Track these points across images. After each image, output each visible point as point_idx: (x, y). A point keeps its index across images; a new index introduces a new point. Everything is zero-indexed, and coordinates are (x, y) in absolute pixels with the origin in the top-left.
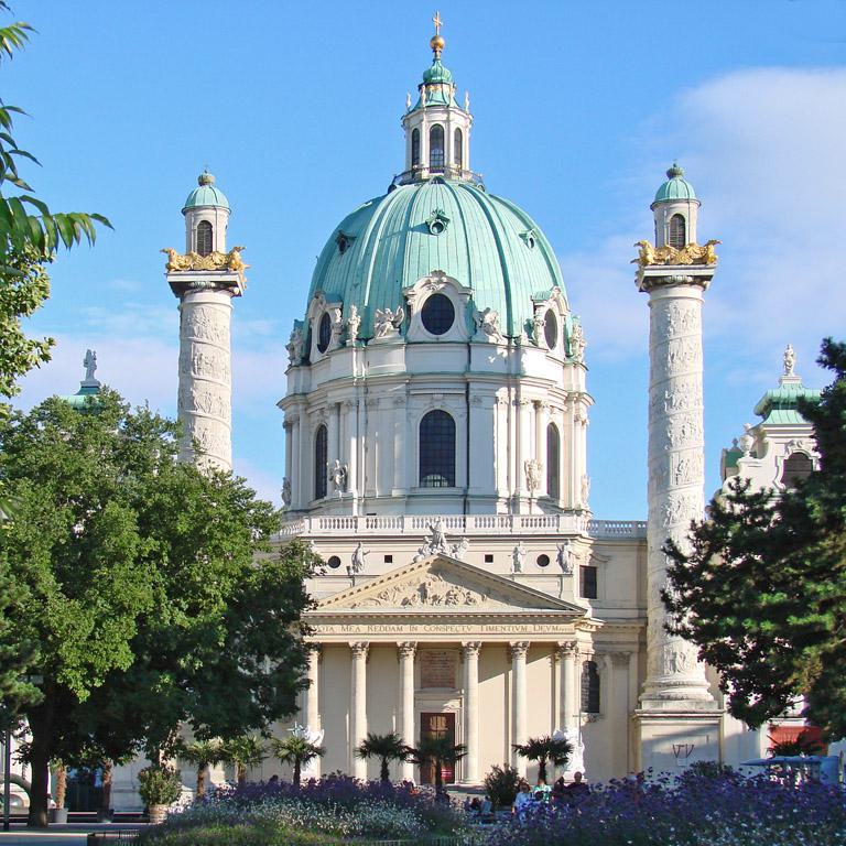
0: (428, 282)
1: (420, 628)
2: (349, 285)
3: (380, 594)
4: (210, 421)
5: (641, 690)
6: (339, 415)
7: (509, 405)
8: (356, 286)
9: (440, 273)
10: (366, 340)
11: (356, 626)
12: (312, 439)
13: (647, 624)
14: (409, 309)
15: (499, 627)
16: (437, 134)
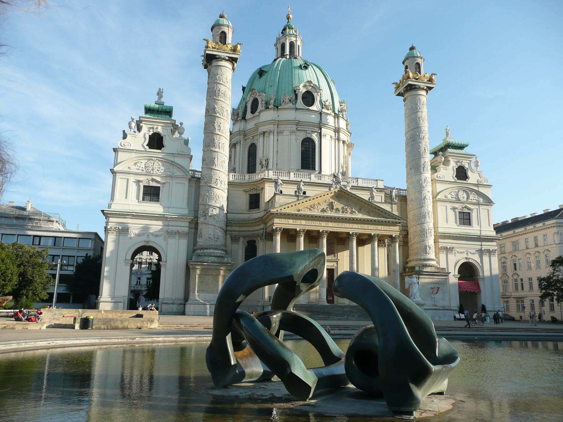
0: (305, 86)
1: (330, 224)
2: (268, 86)
3: (311, 206)
4: (223, 120)
5: (407, 263)
6: (264, 138)
7: (335, 140)
8: (271, 86)
9: (310, 82)
10: (277, 107)
11: (300, 221)
12: (247, 150)
13: (408, 233)
14: (296, 95)
15: (366, 226)
16: (292, 45)
